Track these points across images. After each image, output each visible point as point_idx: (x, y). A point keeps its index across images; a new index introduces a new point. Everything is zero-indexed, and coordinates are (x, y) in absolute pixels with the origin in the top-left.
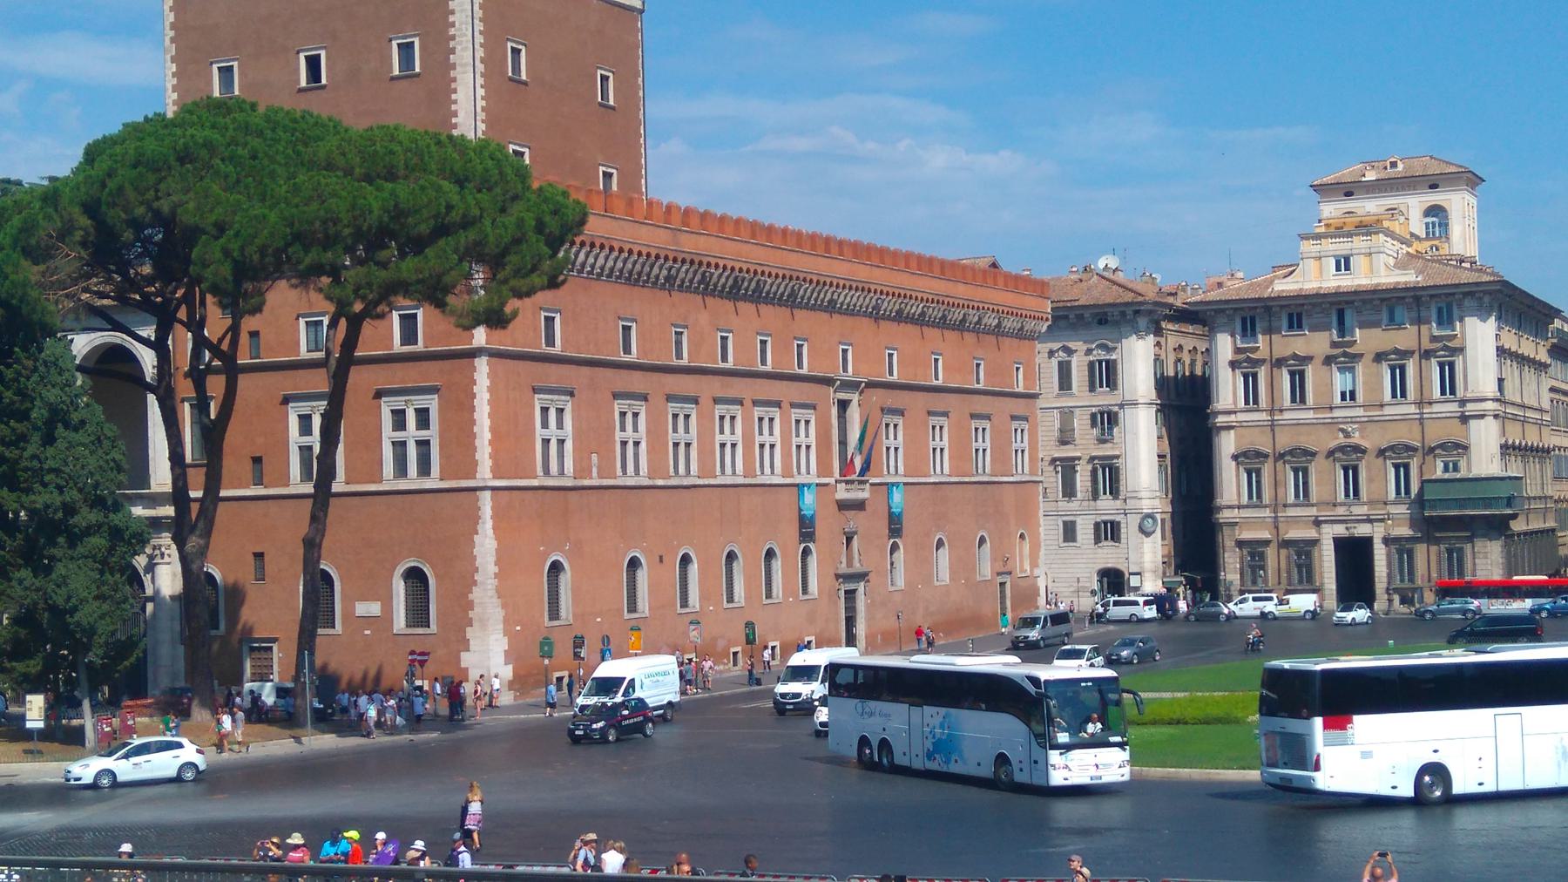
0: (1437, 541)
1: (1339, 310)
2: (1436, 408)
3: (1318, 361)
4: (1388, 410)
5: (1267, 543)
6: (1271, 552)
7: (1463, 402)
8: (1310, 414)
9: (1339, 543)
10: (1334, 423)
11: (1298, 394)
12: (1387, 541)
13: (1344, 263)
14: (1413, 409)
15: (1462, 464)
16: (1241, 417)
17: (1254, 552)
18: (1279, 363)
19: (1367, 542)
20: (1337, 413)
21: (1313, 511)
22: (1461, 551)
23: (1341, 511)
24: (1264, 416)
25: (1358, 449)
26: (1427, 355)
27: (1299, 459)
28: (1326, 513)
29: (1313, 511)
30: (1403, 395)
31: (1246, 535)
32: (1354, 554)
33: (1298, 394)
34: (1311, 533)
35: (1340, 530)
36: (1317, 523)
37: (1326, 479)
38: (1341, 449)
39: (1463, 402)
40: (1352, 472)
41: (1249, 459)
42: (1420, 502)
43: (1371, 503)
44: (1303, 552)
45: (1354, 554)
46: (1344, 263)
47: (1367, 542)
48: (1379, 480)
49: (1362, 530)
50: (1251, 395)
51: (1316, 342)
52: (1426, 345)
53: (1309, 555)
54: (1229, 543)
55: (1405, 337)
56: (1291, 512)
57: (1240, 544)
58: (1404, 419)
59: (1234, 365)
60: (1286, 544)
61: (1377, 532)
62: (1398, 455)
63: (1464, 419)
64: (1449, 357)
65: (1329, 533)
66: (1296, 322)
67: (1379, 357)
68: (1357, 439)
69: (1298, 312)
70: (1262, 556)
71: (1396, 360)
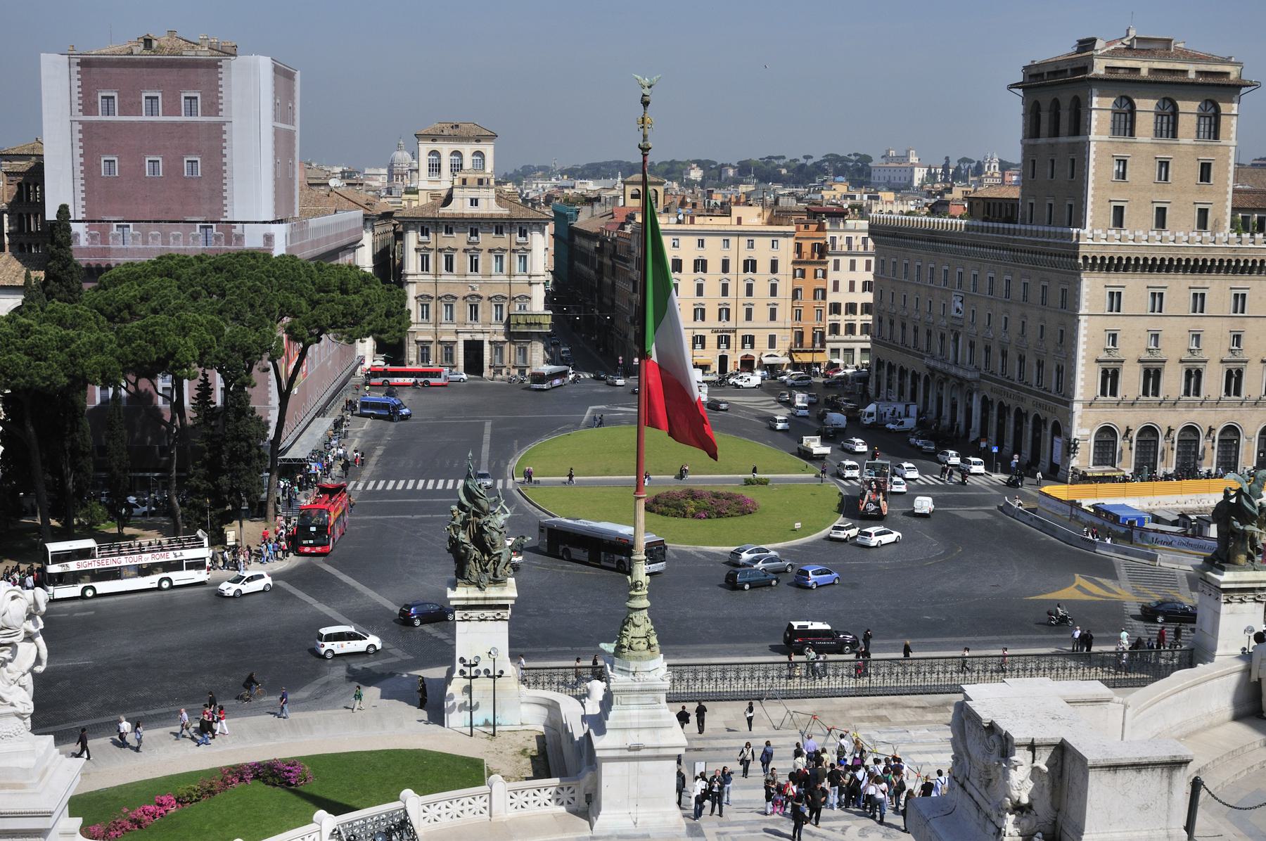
0: (514, 343)
1: (474, 225)
2: (517, 278)
3: (460, 251)
4: (493, 278)
5: (431, 342)
6: (432, 347)
7: (530, 276)
8: (455, 278)
9: (465, 342)
10: (466, 283)
11: (449, 267)
12: (490, 343)
13: (474, 202)
14: (506, 278)
15: (528, 307)
16: (420, 277)
17: (424, 347)
18: (441, 250)
19: (480, 344)
20: (468, 278)
21: (455, 327)
22: (525, 349)
23: (469, 327)
24: (431, 278)
25: (478, 296)
26: (514, 251)
27: (449, 301)
28: (460, 329)
29: (455, 327)
30: (501, 270)
31: (420, 338)
32: (474, 349)
33: (449, 267)
34: (453, 338)
35: (468, 337)
36: (457, 333)
37: (461, 310)
38: (471, 296)
39: (530, 276)
40: (474, 310)
41: (424, 299)
42: (508, 324)
43: (483, 324)
44: (449, 347)
45: (474, 349)
46: (474, 202)
47: (480, 344)
48: (487, 312)
49: (479, 337)
50: (425, 266)
51: (459, 240)
52: (514, 246)
53: (451, 348)
54: (412, 342)
55: (504, 241)
56: (444, 327)
57: (417, 342)
58: (501, 283)
59: (417, 250)
60: (440, 342)
61: (486, 338)
62: (498, 301)
63: (530, 284)
64: (524, 254)
65: (462, 338)
66: (449, 231)
67: (490, 251)
68: (477, 292)
69: (451, 225)
70: (428, 348)
71: (498, 254)
